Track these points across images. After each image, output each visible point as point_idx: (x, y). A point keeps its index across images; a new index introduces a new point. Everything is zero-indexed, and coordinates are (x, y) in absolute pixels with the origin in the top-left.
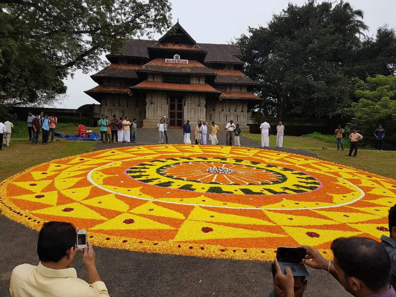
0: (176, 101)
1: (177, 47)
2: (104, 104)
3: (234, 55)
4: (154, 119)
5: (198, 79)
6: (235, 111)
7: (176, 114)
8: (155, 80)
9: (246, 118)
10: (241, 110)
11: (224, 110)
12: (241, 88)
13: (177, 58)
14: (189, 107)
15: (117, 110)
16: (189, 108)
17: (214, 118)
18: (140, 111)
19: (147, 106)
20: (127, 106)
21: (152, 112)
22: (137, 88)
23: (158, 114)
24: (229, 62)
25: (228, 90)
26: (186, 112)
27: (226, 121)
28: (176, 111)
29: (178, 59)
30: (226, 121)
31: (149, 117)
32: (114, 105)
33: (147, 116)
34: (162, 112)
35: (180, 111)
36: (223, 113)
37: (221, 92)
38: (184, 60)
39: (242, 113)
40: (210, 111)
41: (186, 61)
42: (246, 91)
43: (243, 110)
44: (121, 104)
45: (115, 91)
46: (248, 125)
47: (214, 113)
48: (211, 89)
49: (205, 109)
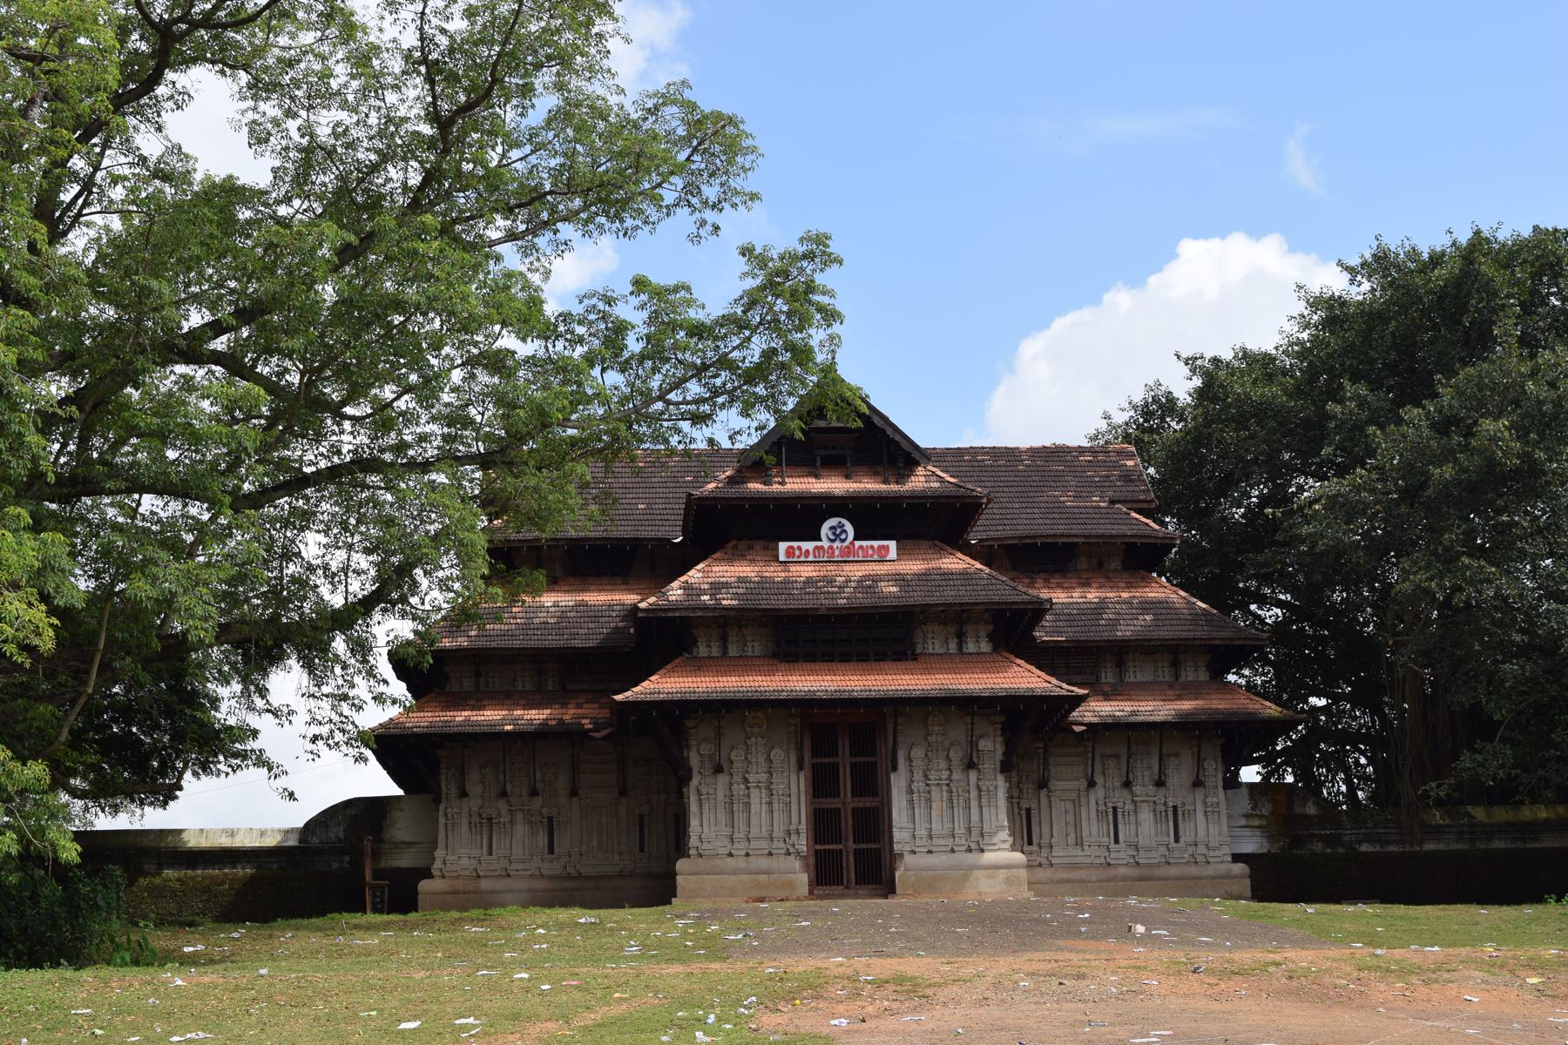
0: (844, 746)
1: (834, 485)
2: (454, 792)
3: (1118, 496)
4: (731, 855)
5: (952, 629)
6: (1160, 783)
7: (847, 822)
8: (733, 651)
9: (1224, 818)
10: (1192, 779)
11: (1099, 780)
12: (1175, 664)
13: (837, 534)
14: (918, 776)
15: (520, 816)
16: (918, 785)
17: (1046, 828)
18: (641, 817)
19: (695, 782)
20: (574, 793)
21: (722, 817)
22: (649, 698)
23: (754, 821)
24: (1097, 536)
25: (1108, 677)
26: (904, 803)
27: (1117, 841)
28: (846, 801)
29: (843, 541)
30: (1112, 845)
31: (705, 846)
32: (503, 794)
33: (693, 841)
34: (776, 814)
35: (867, 802)
36: (1093, 803)
37: (1082, 692)
38: (876, 543)
39: (1199, 794)
40: (1021, 791)
41: (887, 548)
44: (539, 786)
45: (514, 721)
46: (1237, 858)
47: (1044, 801)
48: (1024, 679)
49: (1001, 783)
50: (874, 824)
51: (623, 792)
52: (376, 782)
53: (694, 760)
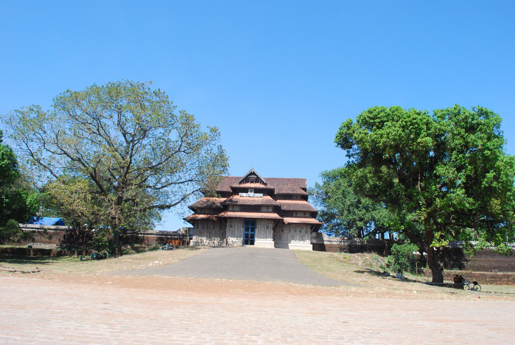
25: (294, 215)
28: (250, 233)
35: (252, 233)
42: (309, 216)
48: (275, 216)
49: (272, 231)
50: (253, 236)
51: (221, 229)
52: (190, 226)
53: (227, 224)
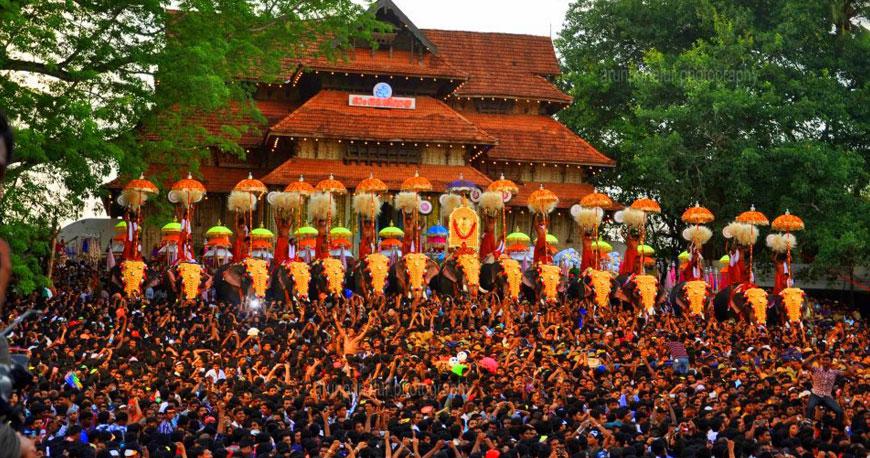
5: (443, 152)
8: (321, 156)
41: (409, 103)
43: (571, 238)
44: (202, 221)
